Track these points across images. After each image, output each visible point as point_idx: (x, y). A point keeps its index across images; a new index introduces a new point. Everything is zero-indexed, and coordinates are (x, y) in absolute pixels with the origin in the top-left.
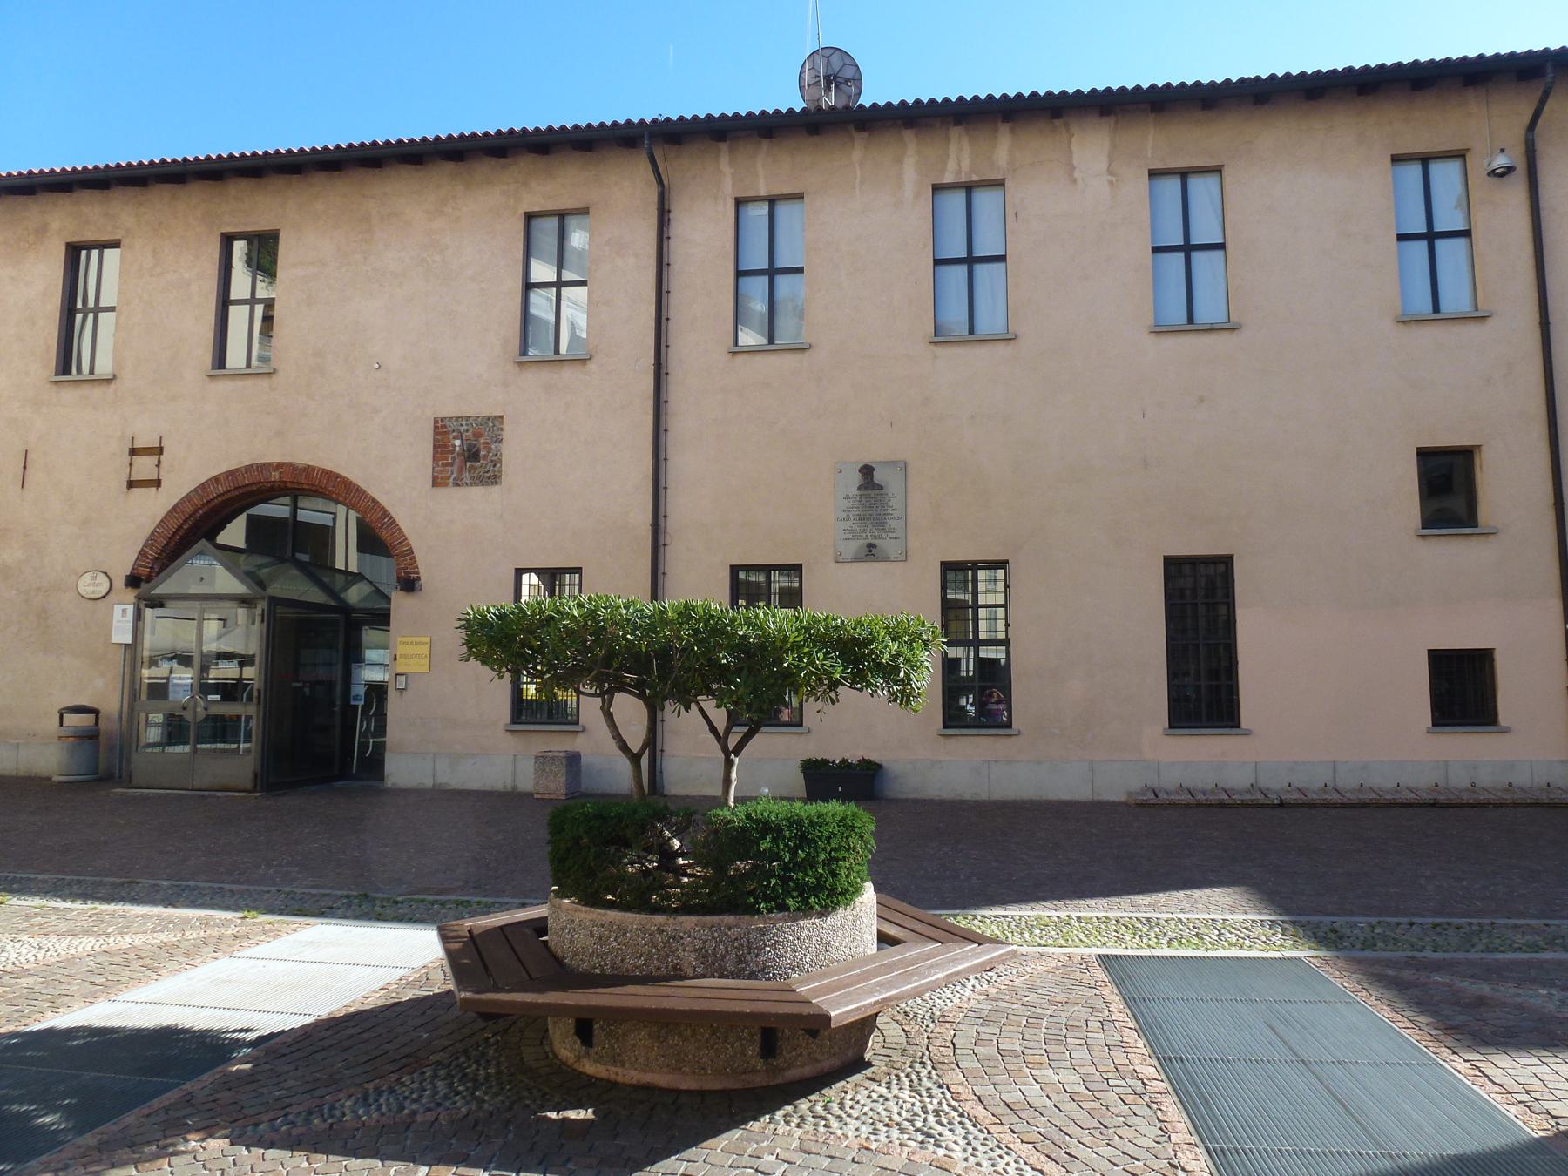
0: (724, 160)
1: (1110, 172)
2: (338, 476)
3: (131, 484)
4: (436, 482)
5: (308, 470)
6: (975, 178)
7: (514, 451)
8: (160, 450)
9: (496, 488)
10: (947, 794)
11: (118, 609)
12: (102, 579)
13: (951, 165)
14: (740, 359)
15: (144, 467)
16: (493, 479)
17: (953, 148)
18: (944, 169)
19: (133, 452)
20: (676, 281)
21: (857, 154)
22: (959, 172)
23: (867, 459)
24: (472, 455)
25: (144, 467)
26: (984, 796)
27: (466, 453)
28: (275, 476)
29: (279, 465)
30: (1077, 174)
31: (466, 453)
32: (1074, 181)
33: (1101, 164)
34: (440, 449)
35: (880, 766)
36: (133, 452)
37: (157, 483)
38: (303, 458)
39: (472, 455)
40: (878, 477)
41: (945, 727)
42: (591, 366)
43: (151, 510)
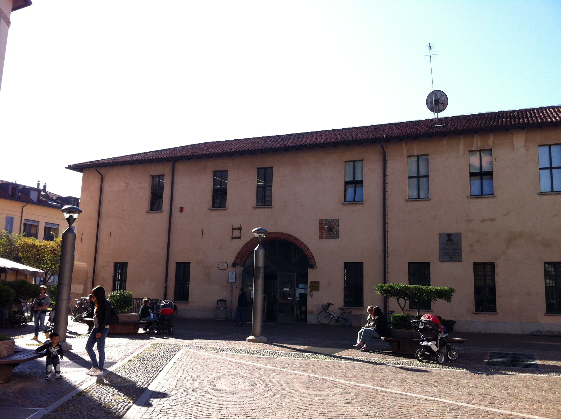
0: (404, 145)
1: (525, 146)
2: (291, 236)
3: (233, 238)
4: (321, 237)
5: (283, 234)
6: (482, 149)
7: (343, 229)
8: (240, 229)
9: (337, 240)
10: (476, 331)
11: (230, 273)
12: (225, 264)
13: (475, 145)
14: (409, 203)
15: (236, 233)
16: (337, 237)
17: (475, 139)
18: (472, 146)
19: (233, 229)
20: (389, 180)
21: (445, 142)
22: (477, 147)
23: (449, 231)
24: (330, 229)
25: (236, 233)
26: (488, 332)
27: (329, 229)
28: (274, 236)
29: (275, 233)
30: (515, 147)
31: (329, 229)
32: (514, 149)
33: (523, 144)
34: (321, 228)
35: (455, 322)
36: (233, 229)
37: (240, 238)
38: (282, 231)
39: (330, 229)
40: (453, 238)
41: (476, 311)
42: (364, 205)
43: (239, 245)
